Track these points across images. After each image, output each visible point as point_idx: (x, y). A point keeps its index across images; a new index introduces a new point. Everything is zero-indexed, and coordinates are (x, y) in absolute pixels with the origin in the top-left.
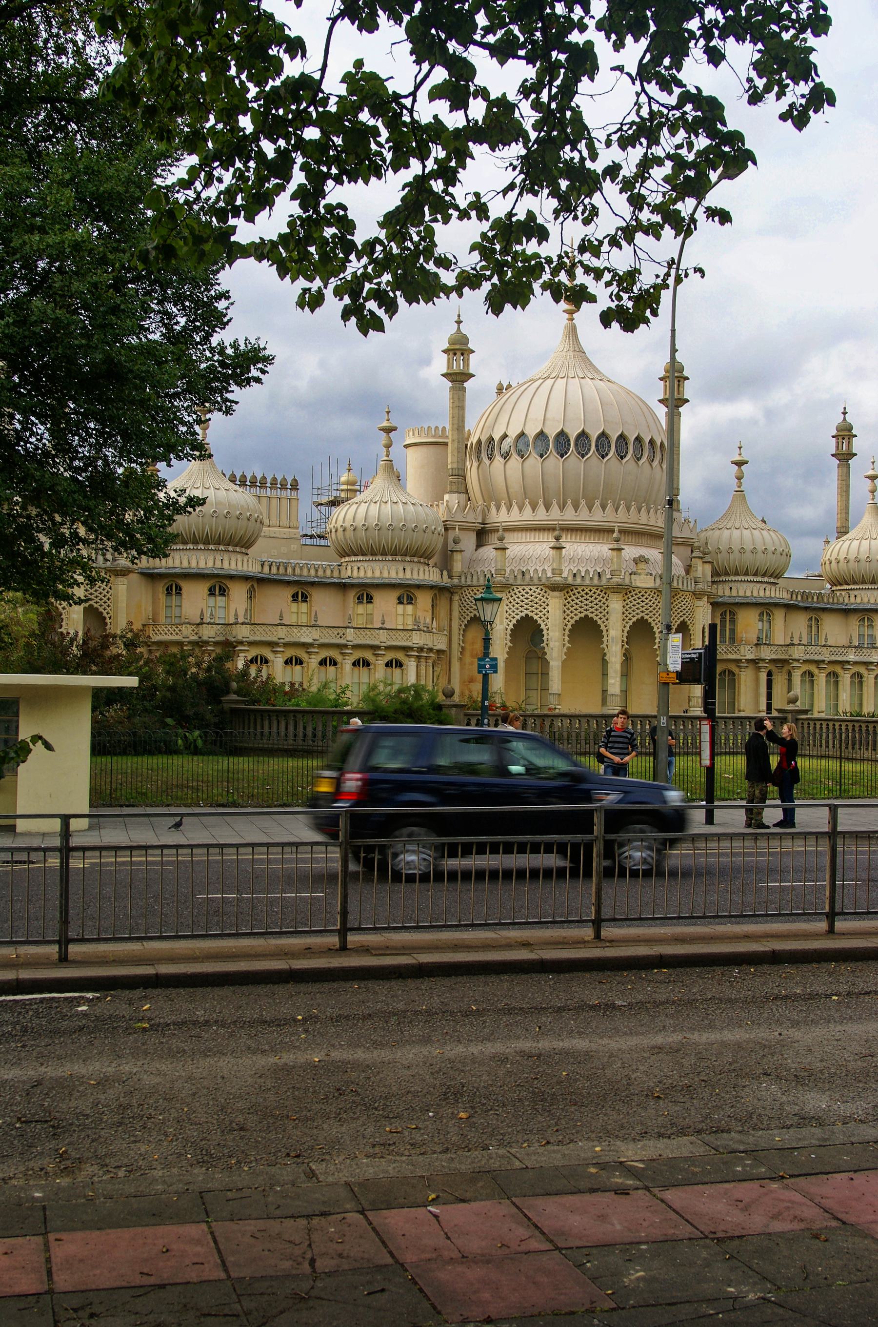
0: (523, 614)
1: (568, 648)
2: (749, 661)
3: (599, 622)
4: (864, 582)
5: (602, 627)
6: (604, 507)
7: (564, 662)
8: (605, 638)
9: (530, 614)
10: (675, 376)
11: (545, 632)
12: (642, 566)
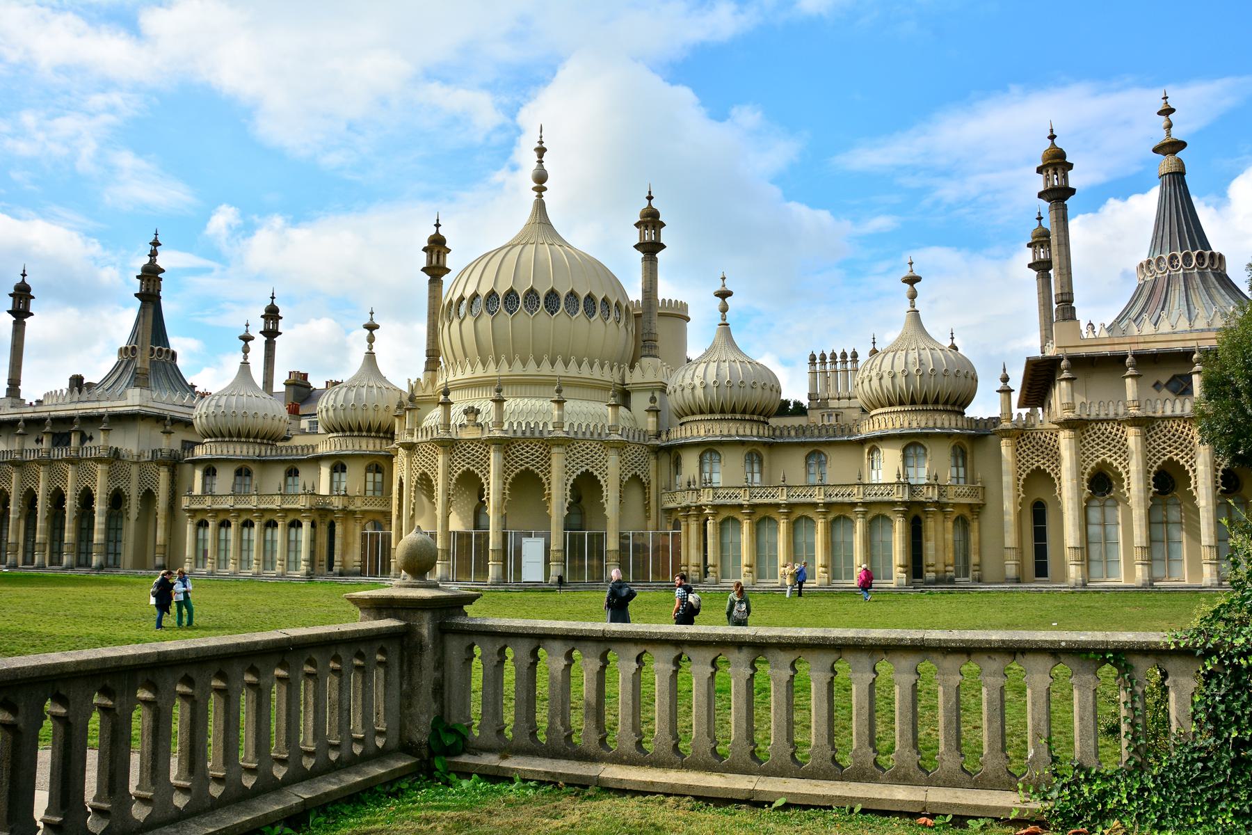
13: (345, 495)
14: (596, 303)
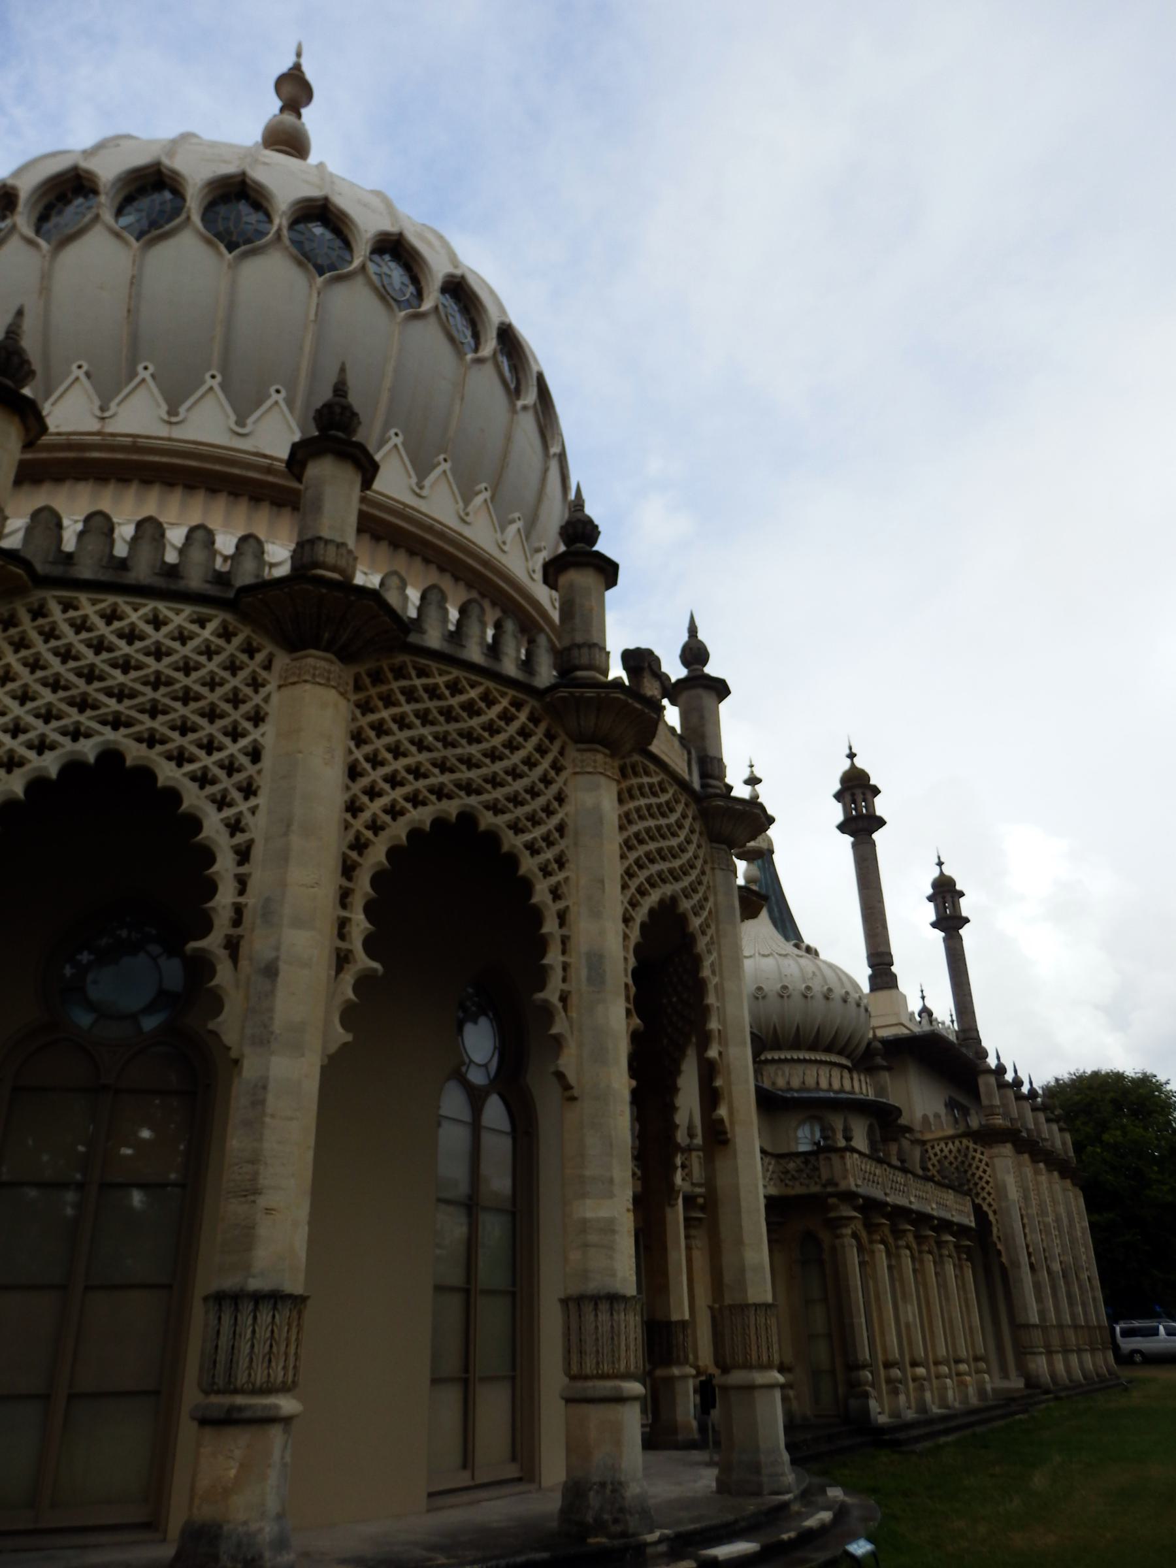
0: (88, 749)
1: (364, 983)
3: (528, 865)
4: (796, 1045)
7: (335, 1069)
8: (553, 957)
9: (135, 752)
11: (225, 865)
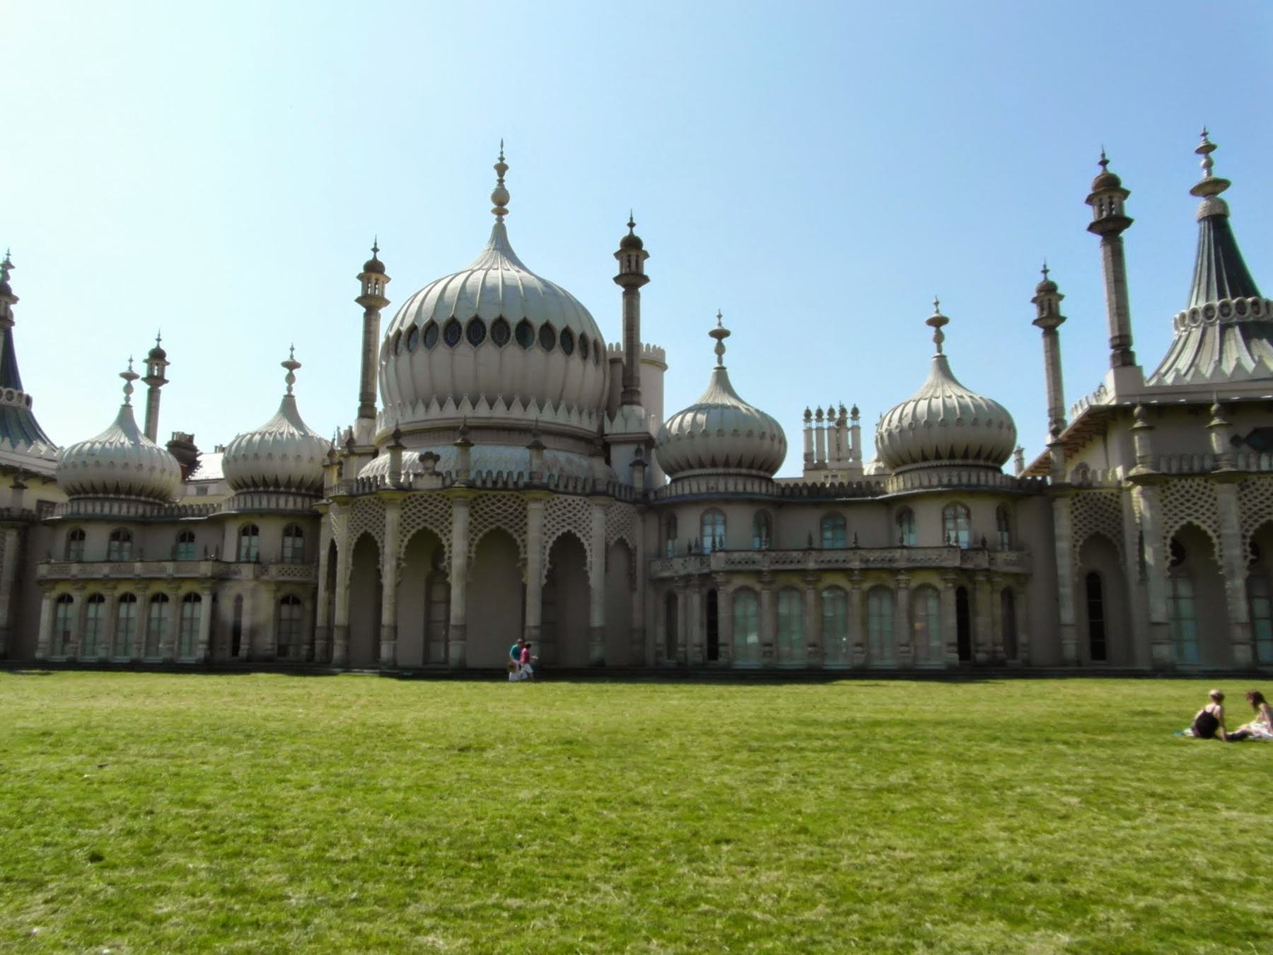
2: (681, 578)
5: (379, 545)
6: (556, 409)
10: (632, 250)
12: (430, 463)
13: (257, 562)
14: (563, 334)
